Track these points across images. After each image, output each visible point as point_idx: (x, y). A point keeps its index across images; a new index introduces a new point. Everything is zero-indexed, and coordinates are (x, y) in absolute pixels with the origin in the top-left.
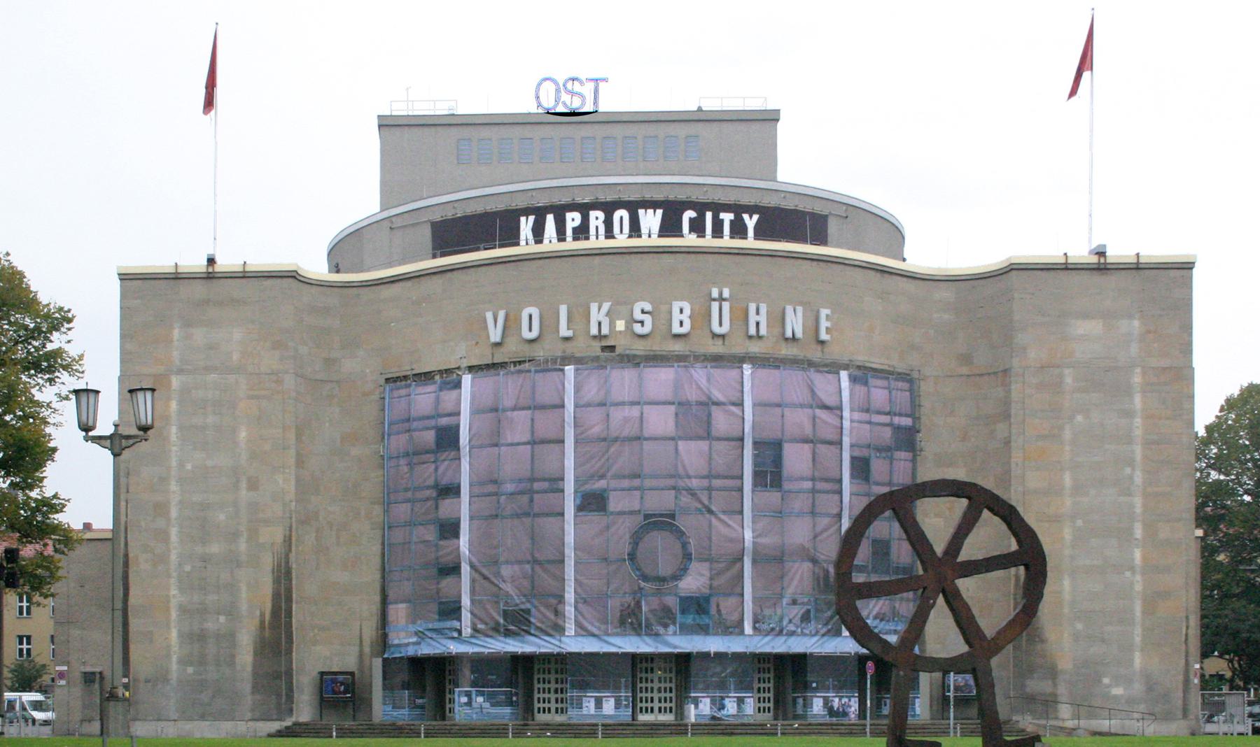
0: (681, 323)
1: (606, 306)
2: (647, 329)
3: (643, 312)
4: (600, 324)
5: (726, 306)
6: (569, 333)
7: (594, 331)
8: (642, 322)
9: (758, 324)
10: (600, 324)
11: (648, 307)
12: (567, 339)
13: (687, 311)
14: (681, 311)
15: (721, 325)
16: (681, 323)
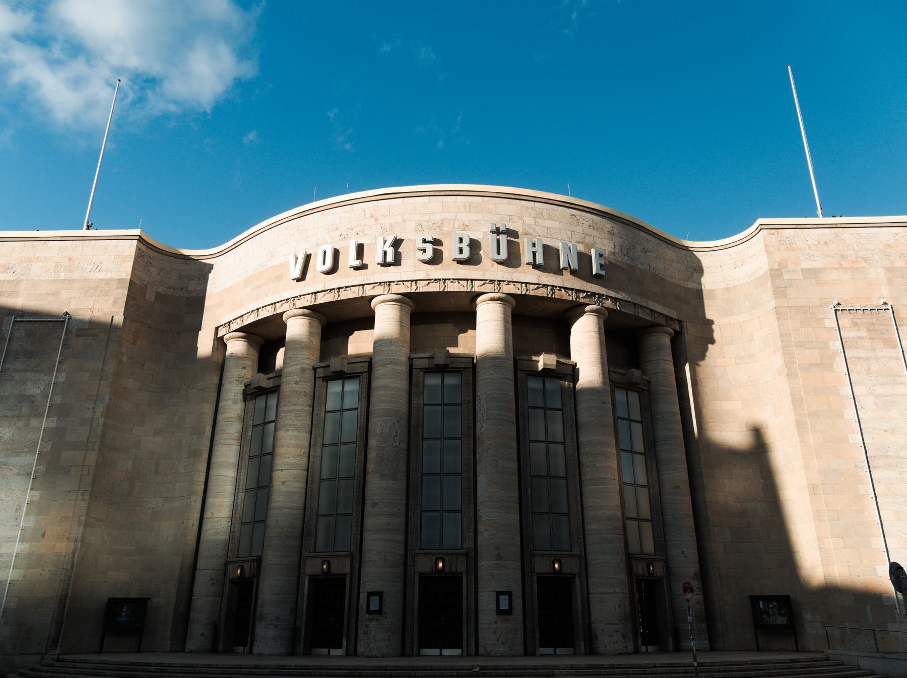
0: (461, 251)
1: (390, 240)
2: (429, 255)
3: (425, 241)
4: (385, 253)
5: (503, 238)
6: (358, 263)
7: (380, 259)
8: (424, 250)
9: (534, 254)
10: (385, 253)
11: (429, 238)
12: (356, 268)
13: (466, 241)
14: (461, 240)
15: (499, 253)
16: (461, 251)
